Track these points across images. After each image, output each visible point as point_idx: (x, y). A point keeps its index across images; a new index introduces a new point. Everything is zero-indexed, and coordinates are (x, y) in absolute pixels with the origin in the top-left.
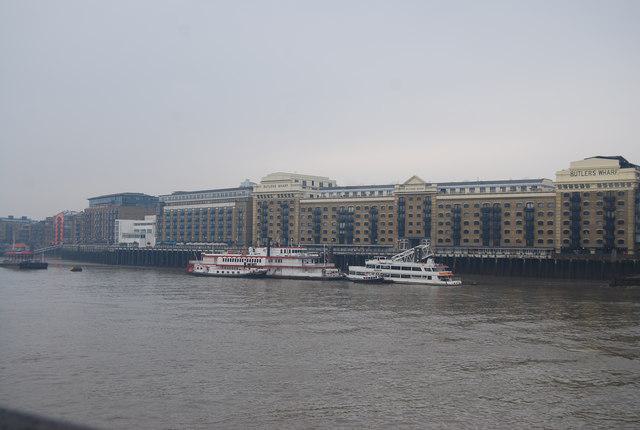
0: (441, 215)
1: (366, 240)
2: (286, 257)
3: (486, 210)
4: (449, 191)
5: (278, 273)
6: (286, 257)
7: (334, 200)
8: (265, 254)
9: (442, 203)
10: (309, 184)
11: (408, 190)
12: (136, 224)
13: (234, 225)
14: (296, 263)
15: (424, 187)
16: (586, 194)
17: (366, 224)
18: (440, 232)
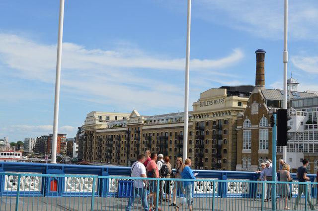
3: (161, 138)
9: (145, 132)
10: (112, 118)
16: (207, 123)
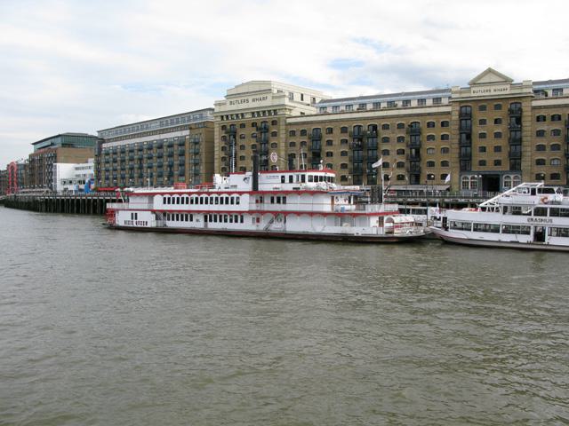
0: (540, 134)
1: (400, 178)
2: (297, 192)
4: (550, 93)
5: (277, 227)
6: (297, 192)
7: (342, 116)
8: (248, 187)
9: (543, 113)
10: (297, 98)
11: (479, 93)
12: (77, 169)
13: (187, 161)
14: (325, 205)
15: (508, 86)
17: (401, 152)
18: (540, 162)
